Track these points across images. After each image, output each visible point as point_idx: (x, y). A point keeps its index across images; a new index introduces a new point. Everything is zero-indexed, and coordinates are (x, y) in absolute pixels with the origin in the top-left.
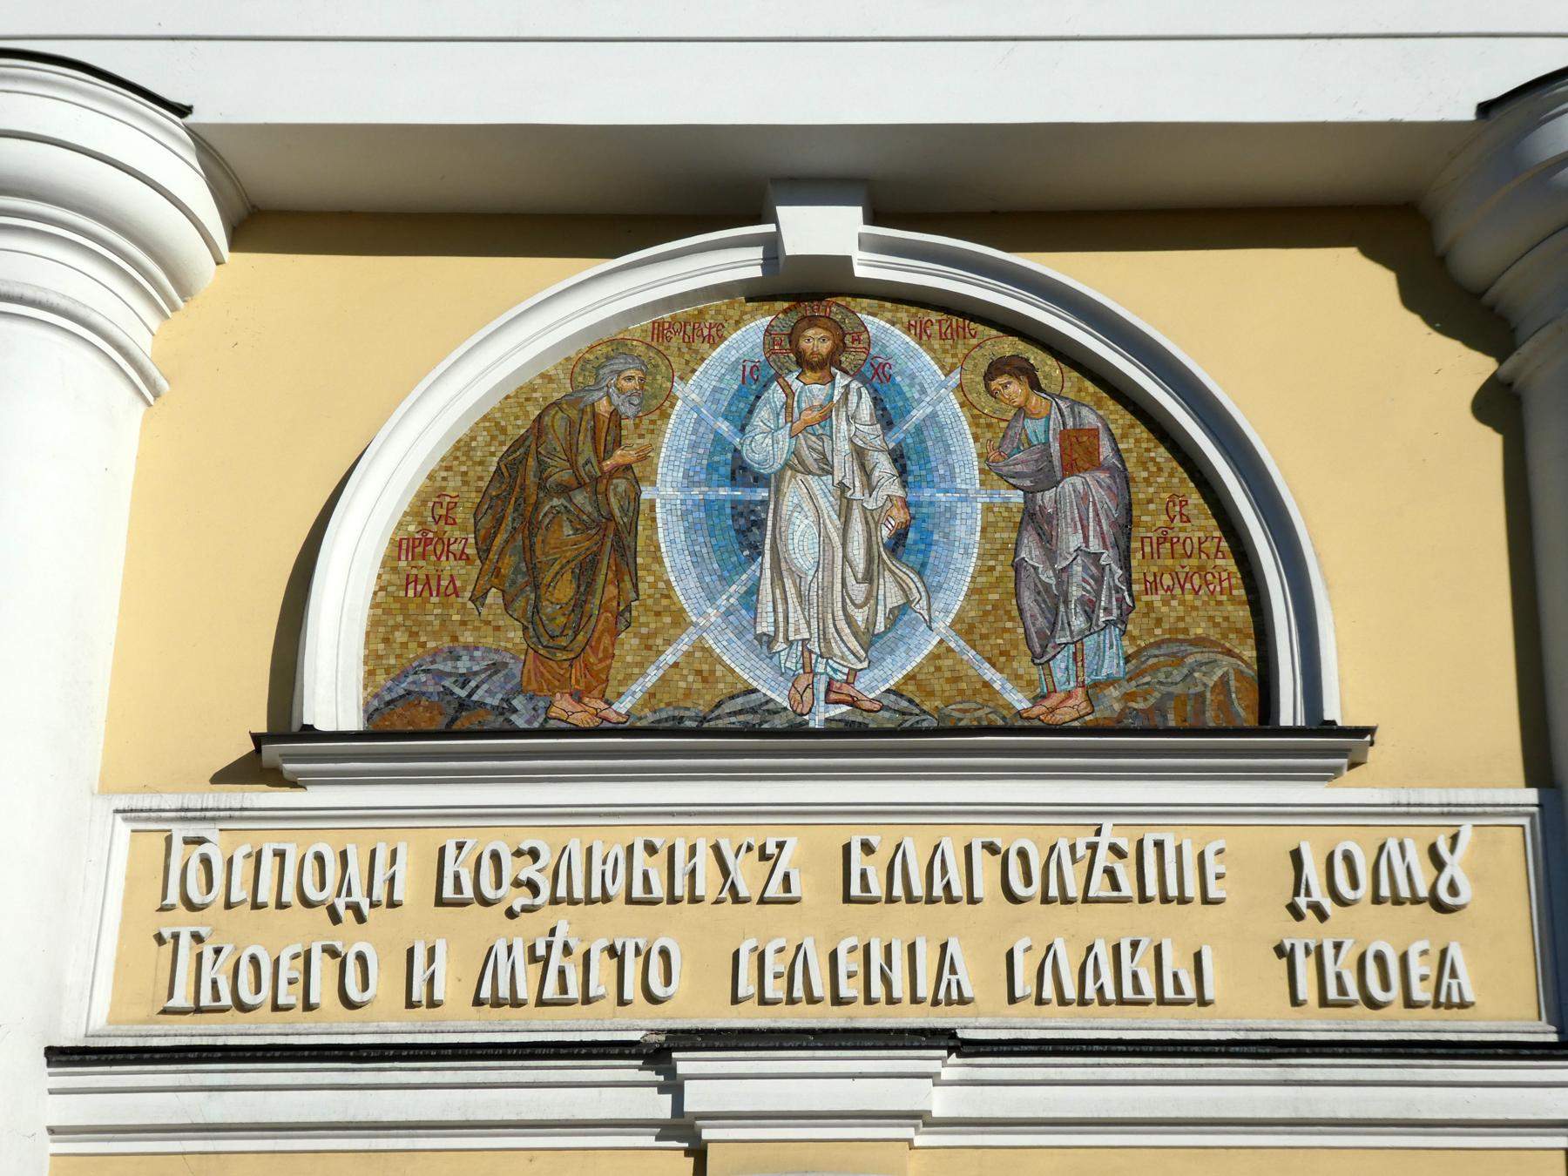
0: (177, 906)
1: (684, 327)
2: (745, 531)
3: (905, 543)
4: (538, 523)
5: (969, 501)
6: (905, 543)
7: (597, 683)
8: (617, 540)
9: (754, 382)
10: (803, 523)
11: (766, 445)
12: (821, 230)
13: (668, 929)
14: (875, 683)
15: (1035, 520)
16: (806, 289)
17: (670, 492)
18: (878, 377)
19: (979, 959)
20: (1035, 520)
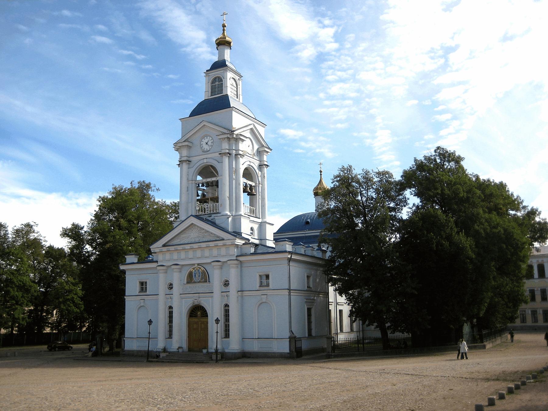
1: (194, 269)
2: (195, 276)
5: (201, 274)
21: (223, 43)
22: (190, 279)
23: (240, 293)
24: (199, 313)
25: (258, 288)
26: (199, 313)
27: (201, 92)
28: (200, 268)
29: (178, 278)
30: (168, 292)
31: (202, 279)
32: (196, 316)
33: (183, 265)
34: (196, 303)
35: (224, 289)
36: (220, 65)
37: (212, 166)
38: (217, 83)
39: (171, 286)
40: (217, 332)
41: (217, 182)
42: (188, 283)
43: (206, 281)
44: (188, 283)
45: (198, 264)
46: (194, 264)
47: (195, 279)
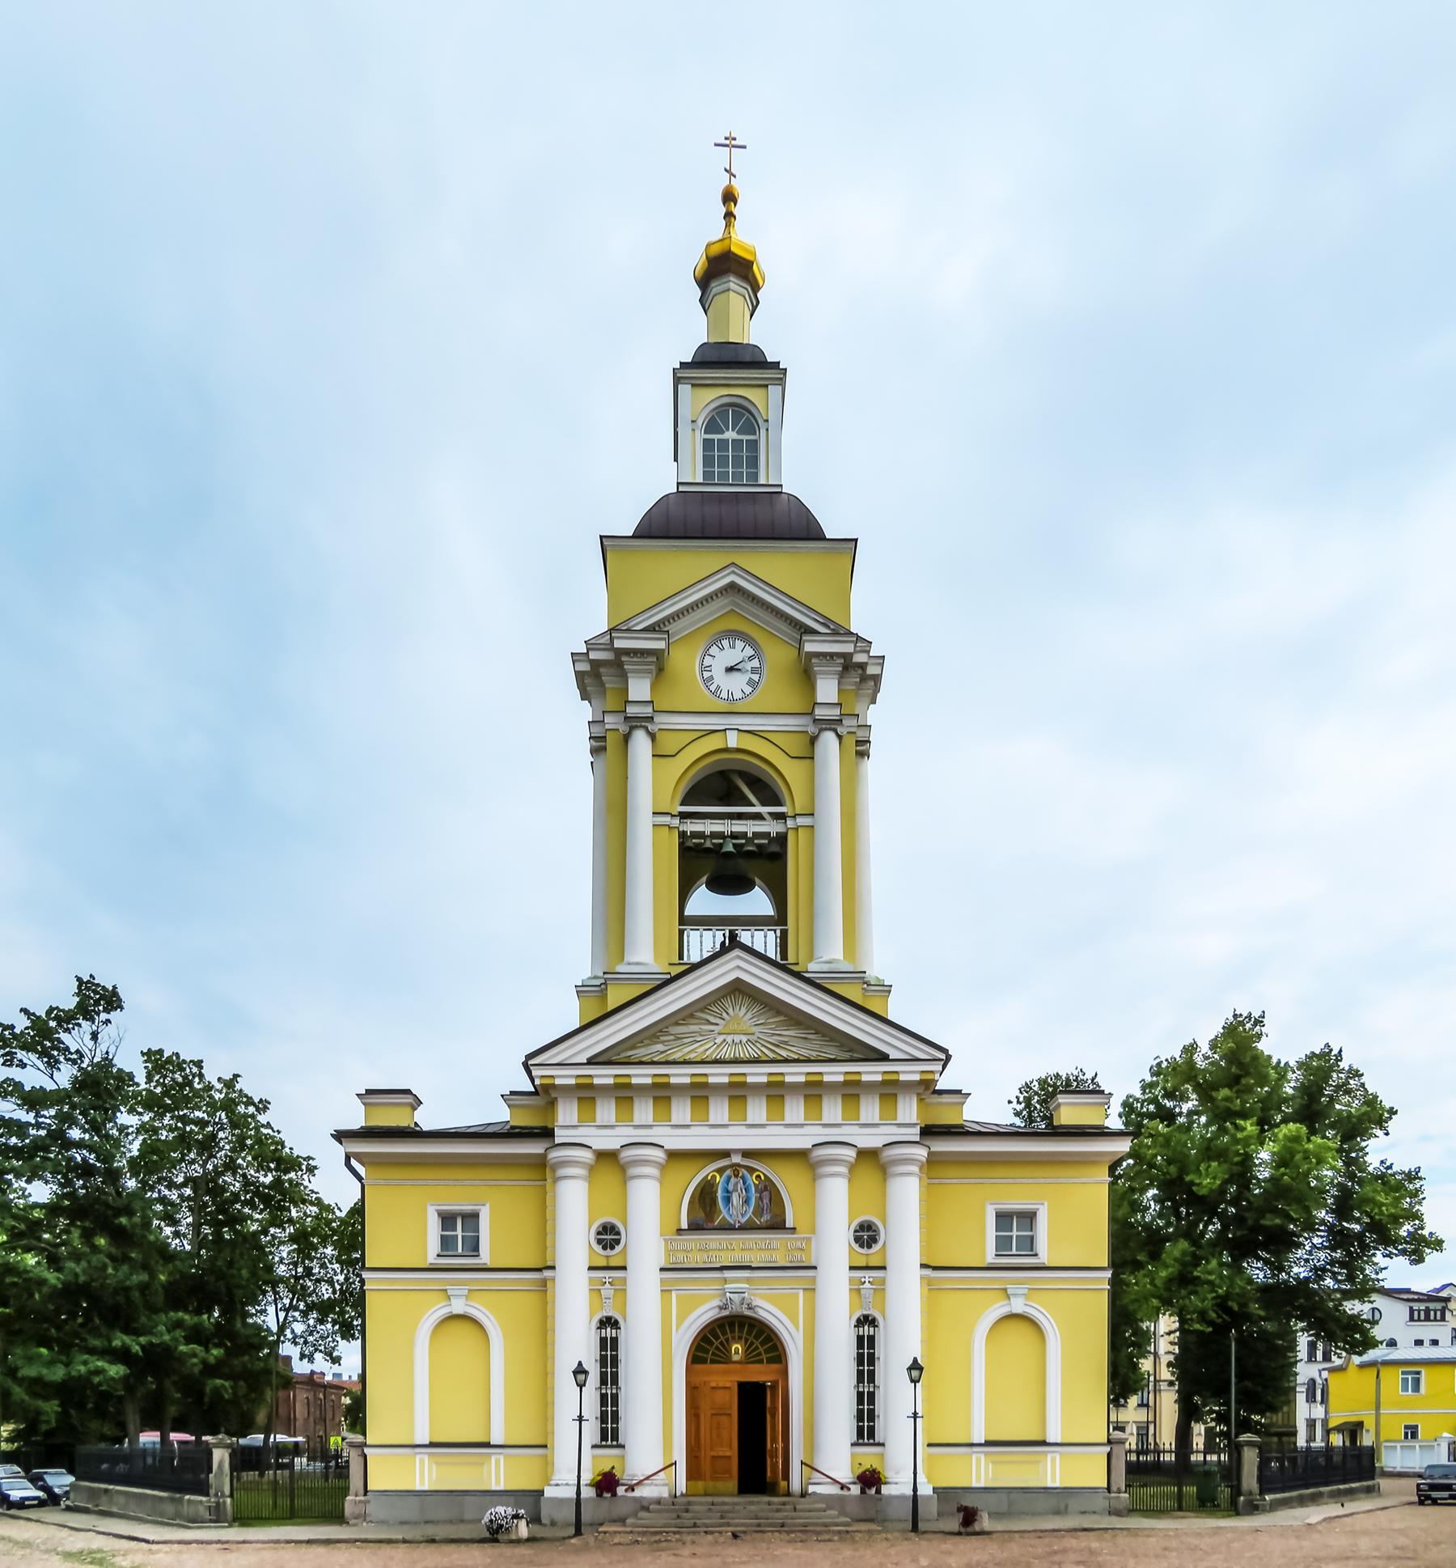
0: (669, 1252)
1: (720, 1171)
3: (747, 1202)
4: (705, 1197)
6: (747, 1202)
7: (712, 1221)
8: (714, 1201)
9: (729, 1178)
10: (735, 1198)
11: (730, 1188)
12: (736, 1159)
13: (722, 1254)
14: (743, 1220)
15: (761, 1198)
16: (736, 1168)
17: (720, 1194)
18: (743, 1178)
19: (756, 1259)
20: (761, 1198)
21: (725, 268)
22: (705, 1213)
23: (928, 1272)
24: (737, 1349)
25: (990, 1258)
26: (737, 1349)
27: (648, 463)
28: (751, 1170)
29: (650, 1209)
30: (601, 1256)
31: (759, 1211)
32: (723, 1357)
33: (674, 1155)
34: (736, 1308)
35: (863, 1256)
36: (728, 363)
37: (743, 774)
38: (730, 435)
39: (609, 1236)
40: (580, 1419)
41: (782, 839)
42: (695, 1227)
43: (777, 1225)
44: (695, 1227)
45: (747, 1154)
46: (725, 1154)
47: (724, 1214)
